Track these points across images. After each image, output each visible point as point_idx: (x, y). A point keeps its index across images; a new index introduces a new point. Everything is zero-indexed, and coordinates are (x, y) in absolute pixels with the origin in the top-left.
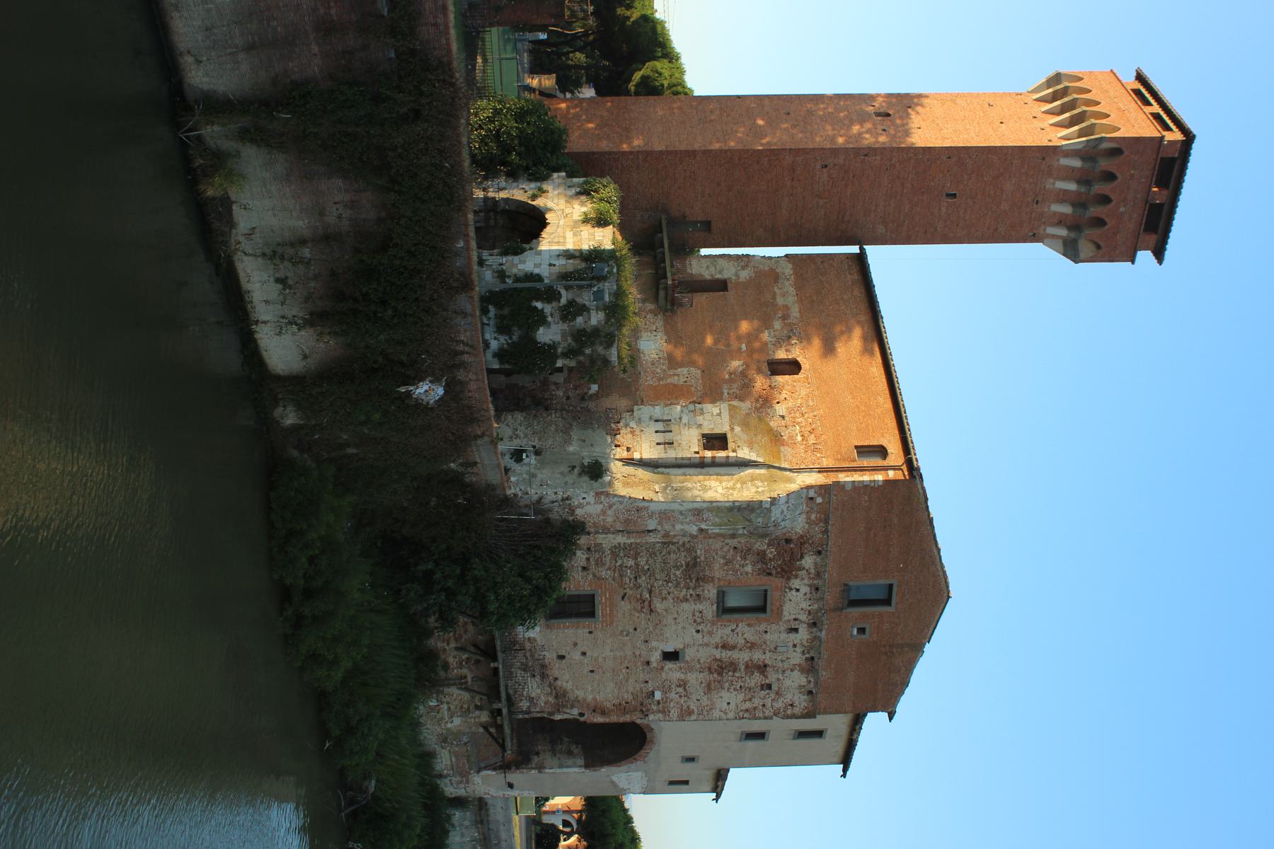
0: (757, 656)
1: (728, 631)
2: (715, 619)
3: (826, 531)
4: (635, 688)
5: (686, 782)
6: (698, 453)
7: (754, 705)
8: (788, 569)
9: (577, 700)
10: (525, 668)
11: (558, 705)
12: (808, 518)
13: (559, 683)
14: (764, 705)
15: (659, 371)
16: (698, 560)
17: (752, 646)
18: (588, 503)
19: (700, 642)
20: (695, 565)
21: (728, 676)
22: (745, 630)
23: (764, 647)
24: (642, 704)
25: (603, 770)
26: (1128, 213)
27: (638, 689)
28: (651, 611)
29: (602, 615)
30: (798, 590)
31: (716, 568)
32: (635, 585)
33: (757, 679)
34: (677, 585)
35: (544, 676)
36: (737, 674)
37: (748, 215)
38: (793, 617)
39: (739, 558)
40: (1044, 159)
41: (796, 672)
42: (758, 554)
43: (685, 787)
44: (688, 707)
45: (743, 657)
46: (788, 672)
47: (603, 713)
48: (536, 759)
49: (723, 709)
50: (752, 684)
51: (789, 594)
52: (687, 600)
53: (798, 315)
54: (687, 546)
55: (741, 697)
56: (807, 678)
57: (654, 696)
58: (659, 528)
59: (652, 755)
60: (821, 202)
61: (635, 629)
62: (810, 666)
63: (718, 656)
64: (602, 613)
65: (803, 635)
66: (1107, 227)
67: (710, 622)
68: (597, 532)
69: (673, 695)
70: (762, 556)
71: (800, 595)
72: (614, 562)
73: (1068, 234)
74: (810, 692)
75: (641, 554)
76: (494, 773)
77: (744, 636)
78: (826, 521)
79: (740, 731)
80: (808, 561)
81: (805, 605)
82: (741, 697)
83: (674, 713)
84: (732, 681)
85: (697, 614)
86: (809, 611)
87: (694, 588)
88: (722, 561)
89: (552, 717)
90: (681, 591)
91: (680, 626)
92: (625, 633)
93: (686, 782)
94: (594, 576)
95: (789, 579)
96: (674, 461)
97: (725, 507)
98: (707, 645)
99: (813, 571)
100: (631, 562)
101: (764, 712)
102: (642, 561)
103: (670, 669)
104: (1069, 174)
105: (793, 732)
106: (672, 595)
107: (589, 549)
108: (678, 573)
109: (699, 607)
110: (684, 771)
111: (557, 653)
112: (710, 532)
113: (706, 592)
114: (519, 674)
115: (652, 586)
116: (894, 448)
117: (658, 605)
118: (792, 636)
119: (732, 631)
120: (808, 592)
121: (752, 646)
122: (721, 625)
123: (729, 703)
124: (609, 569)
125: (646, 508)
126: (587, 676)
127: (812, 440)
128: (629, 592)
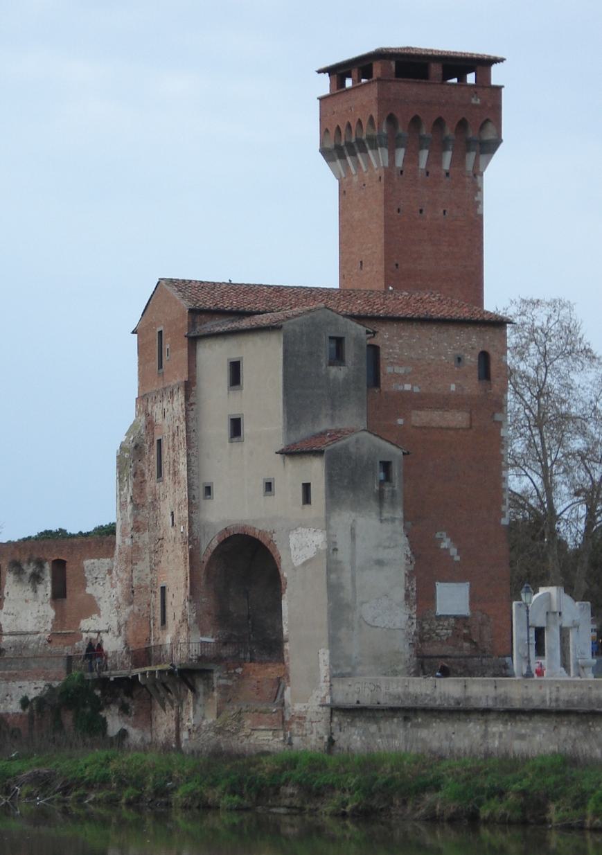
25: (285, 575)
58: (130, 535)
76: (288, 688)
105: (231, 392)
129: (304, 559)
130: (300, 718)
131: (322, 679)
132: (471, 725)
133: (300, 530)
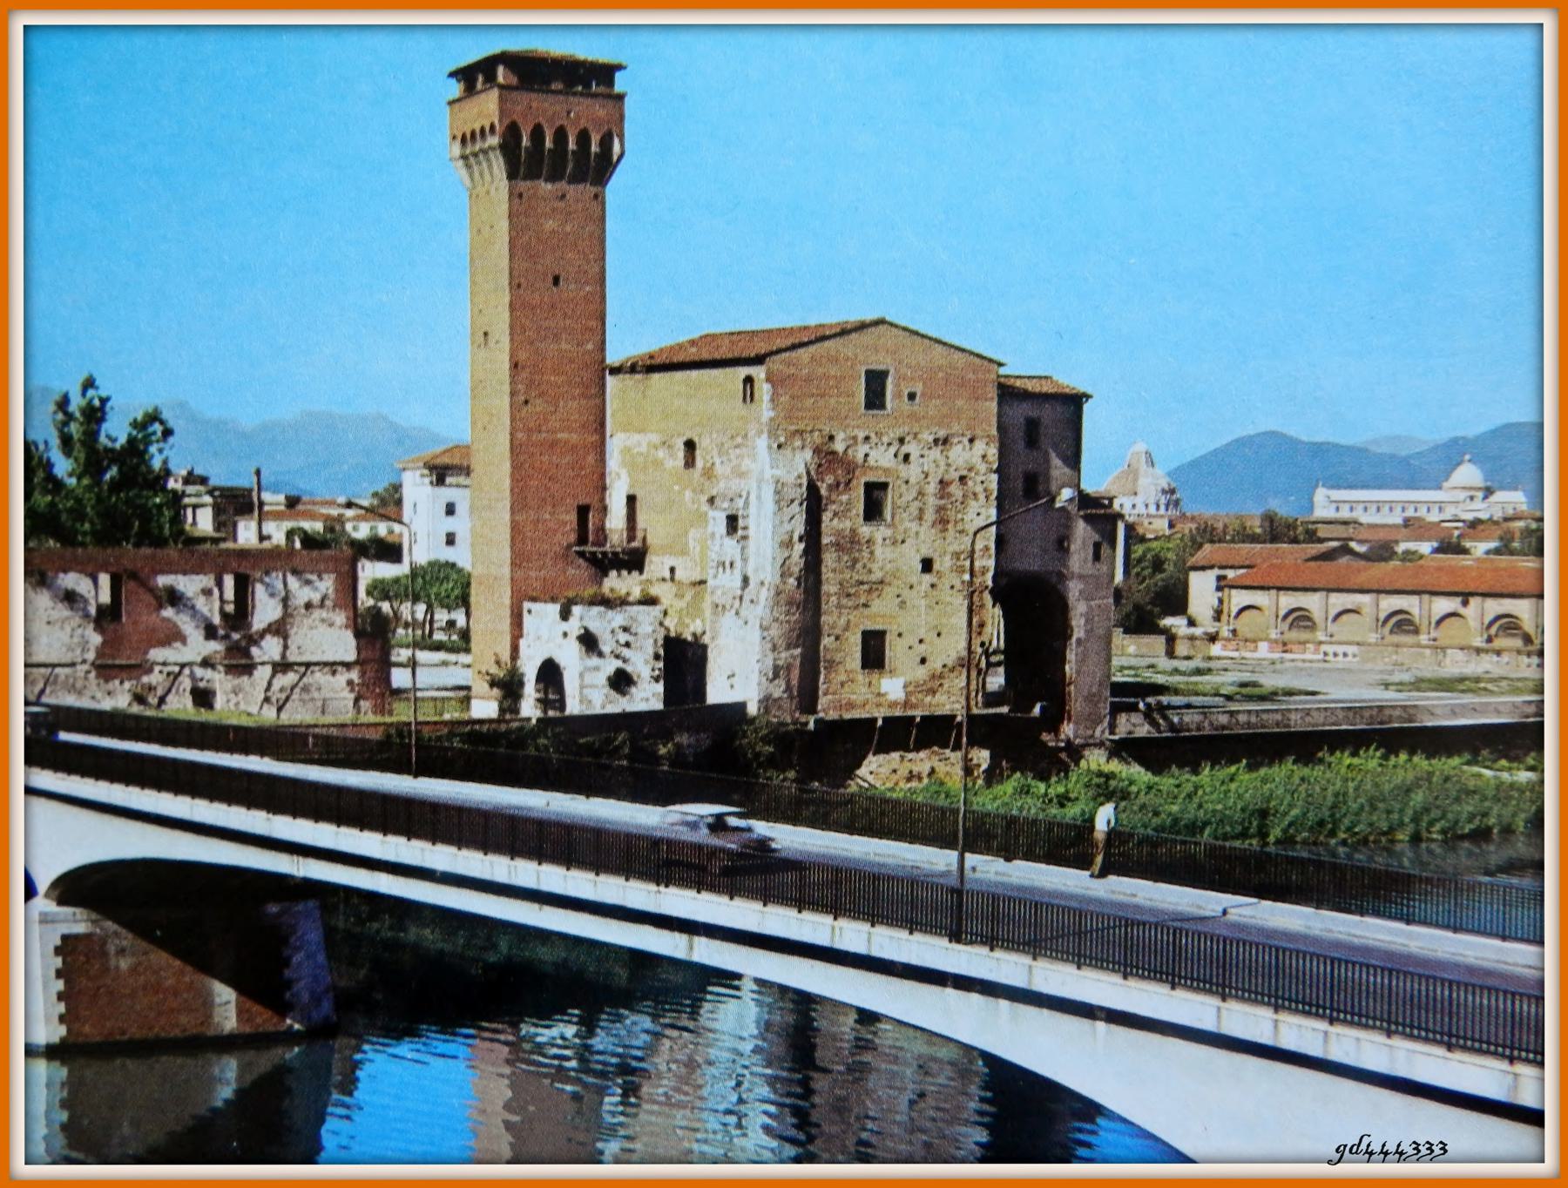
0: (932, 488)
21: (951, 514)
26: (578, 112)
28: (882, 582)
33: (956, 490)
35: (941, 676)
45: (932, 501)
52: (872, 553)
55: (973, 503)
63: (930, 523)
71: (873, 454)
74: (971, 441)
78: (800, 433)
82: (973, 503)
100: (834, 599)
109: (880, 541)
116: (743, 372)
118: (912, 458)
128: (862, 600)
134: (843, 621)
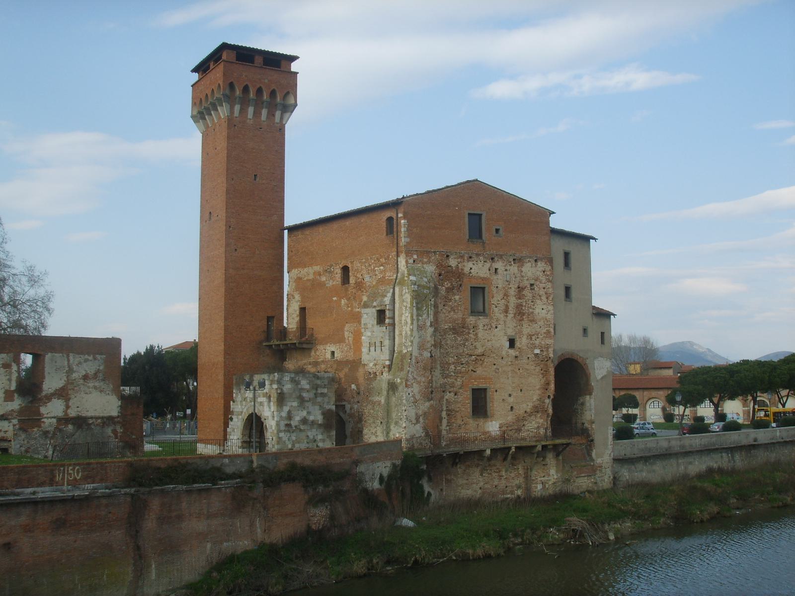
0: (512, 292)
1: (496, 310)
2: (488, 317)
3: (435, 252)
4: (532, 365)
5: (602, 334)
6: (386, 327)
7: (544, 294)
8: (459, 275)
9: (539, 400)
10: (519, 430)
11: (542, 411)
12: (426, 263)
13: (528, 410)
14: (544, 288)
15: (346, 349)
16: (451, 327)
17: (506, 295)
18: (412, 392)
19: (504, 326)
20: (454, 329)
21: (525, 309)
22: (496, 300)
23: (507, 288)
24: (542, 361)
25: (593, 384)
26: (268, 78)
27: (532, 363)
28: (483, 355)
29: (486, 384)
30: (471, 269)
31: (456, 317)
32: (466, 365)
33: (527, 293)
34: (467, 340)
36: (524, 304)
37: (264, 294)
38: (488, 271)
39: (450, 303)
40: (235, 125)
41: (523, 269)
42: (448, 292)
43: (606, 335)
44: (545, 333)
45: (513, 301)
46: (523, 274)
47: (548, 384)
48: (586, 425)
49: (546, 312)
50: (530, 295)
51: (473, 274)
53: (319, 266)
54: (442, 333)
55: (538, 302)
56: (526, 263)
57: (538, 354)
59: (581, 354)
60: (257, 252)
61: (495, 364)
62: (519, 261)
63: (513, 315)
64: (484, 384)
65: (499, 265)
66: (276, 89)
67: (490, 320)
68: (432, 387)
69: (537, 342)
70: (449, 290)
71: (474, 267)
72: (452, 377)
73: (280, 110)
74: (536, 261)
75: (447, 360)
76: (594, 450)
77: (500, 299)
78: (428, 252)
79: (564, 302)
80: (453, 262)
81: (480, 265)
82: (538, 302)
83: (549, 341)
84: (528, 307)
85: (485, 328)
86: (484, 262)
87: (469, 329)
88: (452, 313)
89: (551, 414)
90: (471, 337)
91: (493, 338)
92: (497, 371)
93: (602, 334)
94: (461, 388)
95: (464, 274)
96: (391, 341)
97: (417, 310)
98: (505, 322)
99: (459, 260)
100: (452, 367)
101: (549, 288)
102: (451, 360)
103: (521, 344)
104: (243, 111)
106: (473, 343)
107: (444, 392)
108: (459, 339)
109: (481, 326)
110: (594, 335)
111: (509, 411)
112: (432, 320)
113: (471, 322)
114: (524, 434)
115: (467, 355)
117: (479, 351)
119: (496, 307)
120: (472, 262)
121: (506, 295)
122: (493, 314)
123: (543, 309)
124: (456, 379)
125: (416, 358)
126: (524, 393)
127: (383, 260)
128: (471, 368)
129: (602, 376)
130: (600, 467)
131: (610, 443)
132: (672, 460)
133: (600, 359)
134: (459, 382)
